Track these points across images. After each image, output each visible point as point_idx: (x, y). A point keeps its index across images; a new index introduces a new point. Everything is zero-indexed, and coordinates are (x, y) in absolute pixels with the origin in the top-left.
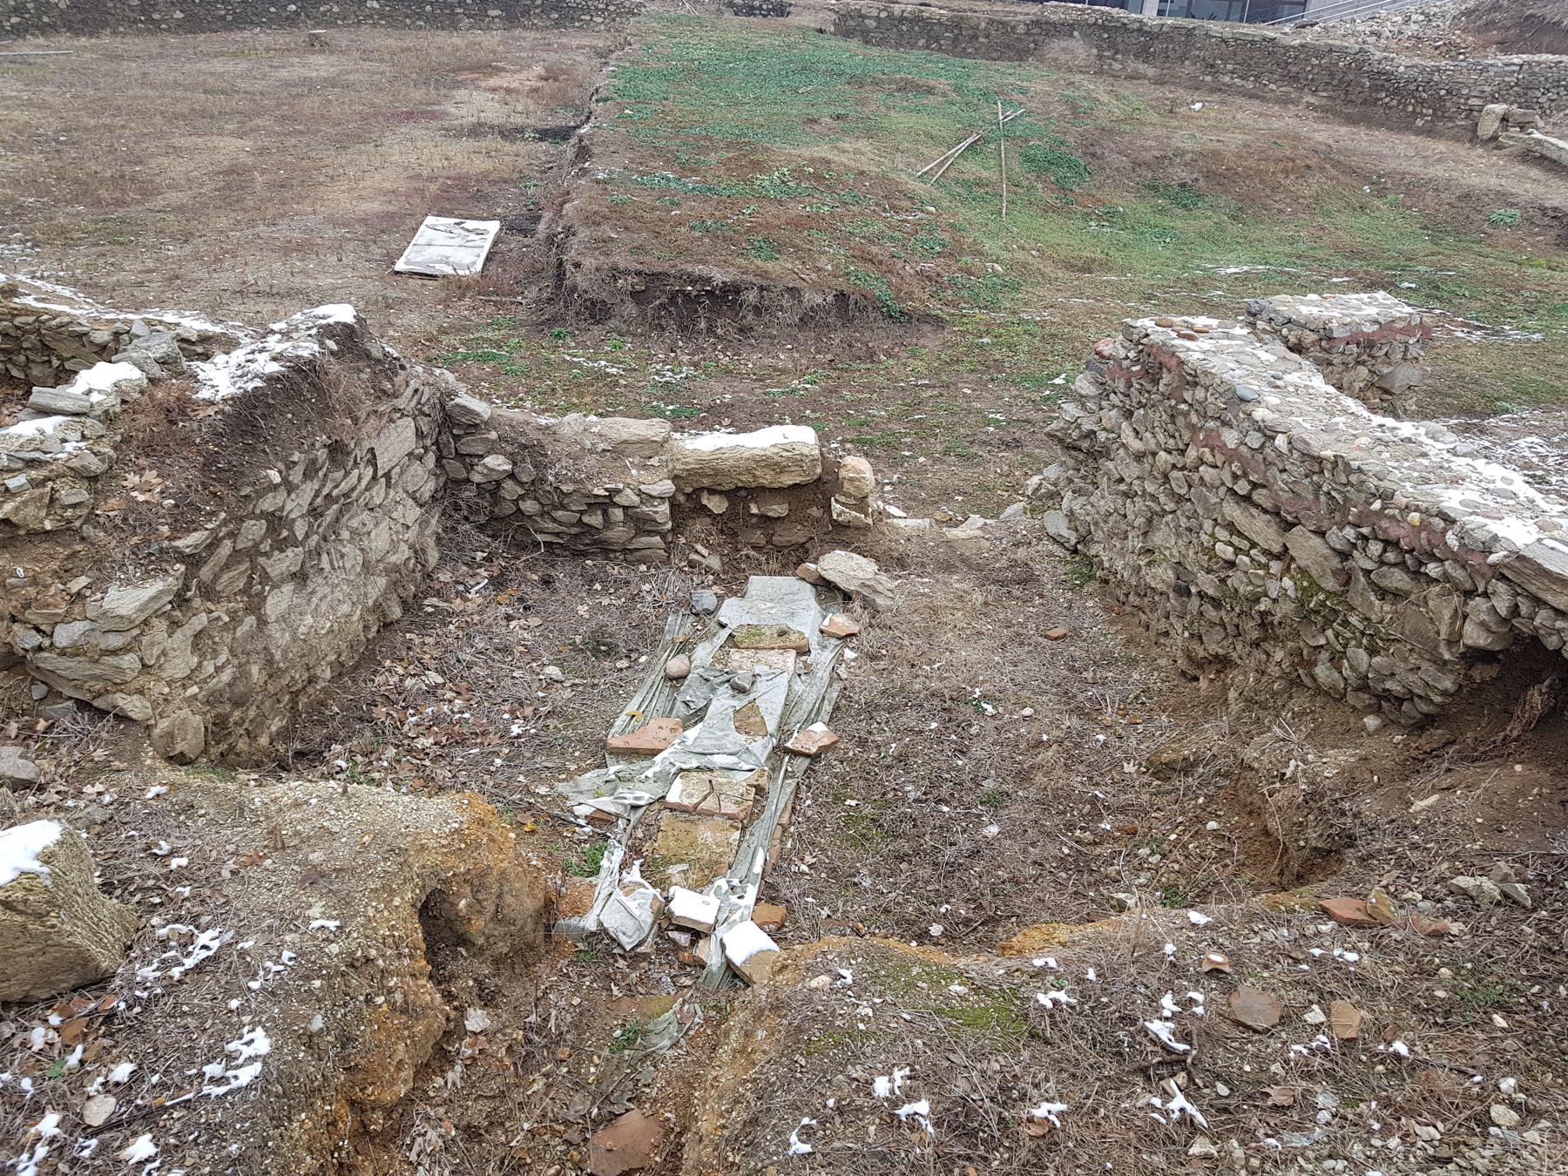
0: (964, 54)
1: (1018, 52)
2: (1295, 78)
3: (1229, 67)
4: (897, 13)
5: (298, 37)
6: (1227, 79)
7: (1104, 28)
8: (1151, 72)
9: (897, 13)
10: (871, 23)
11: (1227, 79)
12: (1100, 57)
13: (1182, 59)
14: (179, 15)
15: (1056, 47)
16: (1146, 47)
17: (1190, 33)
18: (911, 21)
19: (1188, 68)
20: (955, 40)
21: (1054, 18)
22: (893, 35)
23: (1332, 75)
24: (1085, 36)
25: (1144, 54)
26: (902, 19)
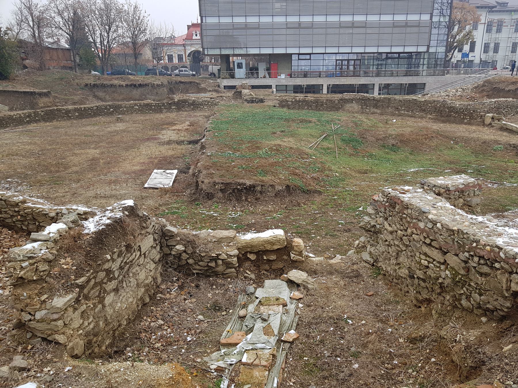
0: (320, 110)
1: (336, 108)
2: (424, 110)
3: (403, 108)
4: (298, 99)
5: (113, 118)
6: (403, 112)
7: (362, 99)
8: (379, 111)
9: (298, 99)
10: (290, 103)
11: (403, 112)
12: (362, 108)
13: (388, 107)
14: (77, 114)
15: (348, 106)
17: (389, 99)
18: (302, 101)
19: (390, 110)
20: (316, 106)
21: (347, 98)
22: (297, 106)
23: (436, 109)
25: (376, 106)
26: (299, 101)
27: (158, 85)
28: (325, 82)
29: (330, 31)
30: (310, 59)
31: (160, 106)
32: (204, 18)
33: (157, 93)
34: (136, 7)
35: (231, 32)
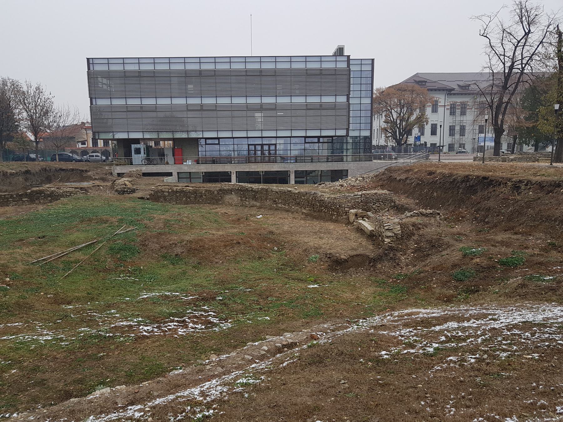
0: (199, 203)
1: (216, 200)
2: (299, 204)
3: (280, 201)
6: (280, 205)
7: (241, 190)
8: (258, 204)
11: (280, 205)
12: (241, 200)
13: (266, 199)
15: (227, 198)
16: (255, 196)
17: (267, 190)
18: (180, 192)
19: (268, 203)
20: (195, 198)
22: (174, 197)
23: (308, 202)
24: (236, 193)
25: (255, 198)
26: (177, 192)
27: (11, 174)
28: (232, 169)
29: (236, 114)
30: (219, 144)
31: (8, 198)
32: (94, 100)
33: (10, 183)
34: (38, 88)
35: (179, 115)
